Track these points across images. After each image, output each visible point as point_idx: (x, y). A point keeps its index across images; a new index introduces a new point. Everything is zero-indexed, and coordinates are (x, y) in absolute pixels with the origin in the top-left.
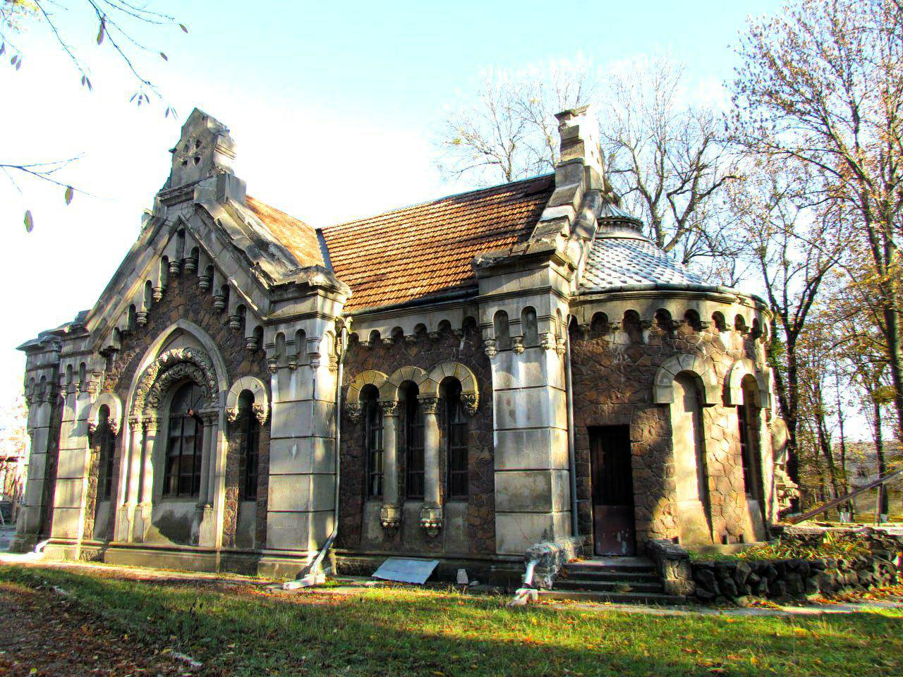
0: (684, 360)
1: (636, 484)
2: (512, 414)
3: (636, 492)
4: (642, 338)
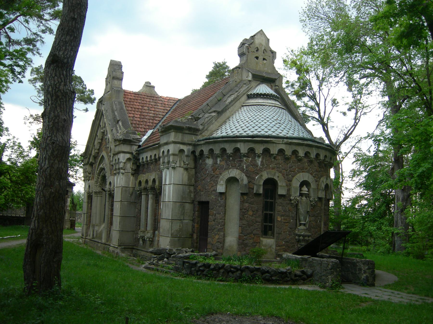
0: (231, 172)
1: (209, 228)
2: (165, 194)
3: (209, 231)
4: (217, 161)
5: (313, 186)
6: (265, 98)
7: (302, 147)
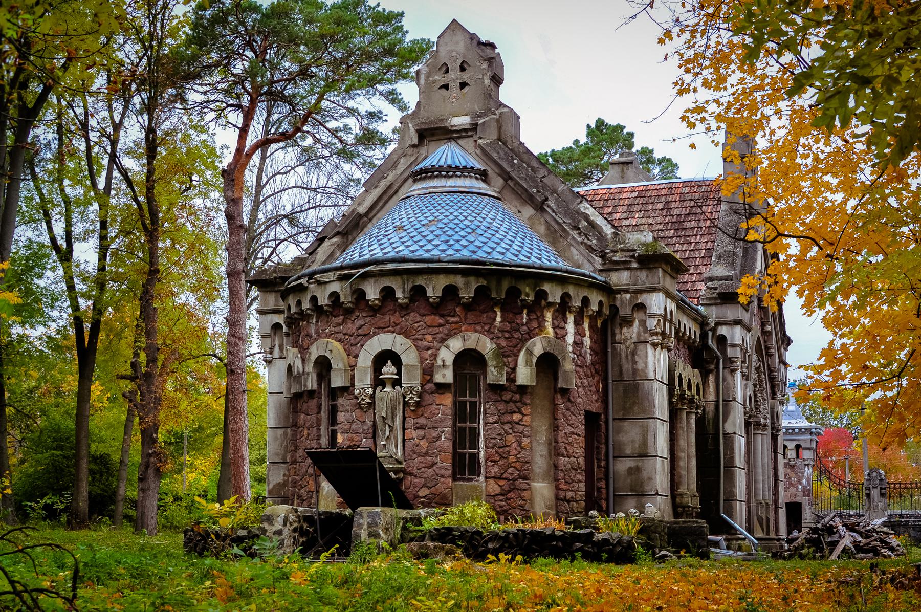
5: (409, 358)
6: (425, 178)
7: (372, 280)
